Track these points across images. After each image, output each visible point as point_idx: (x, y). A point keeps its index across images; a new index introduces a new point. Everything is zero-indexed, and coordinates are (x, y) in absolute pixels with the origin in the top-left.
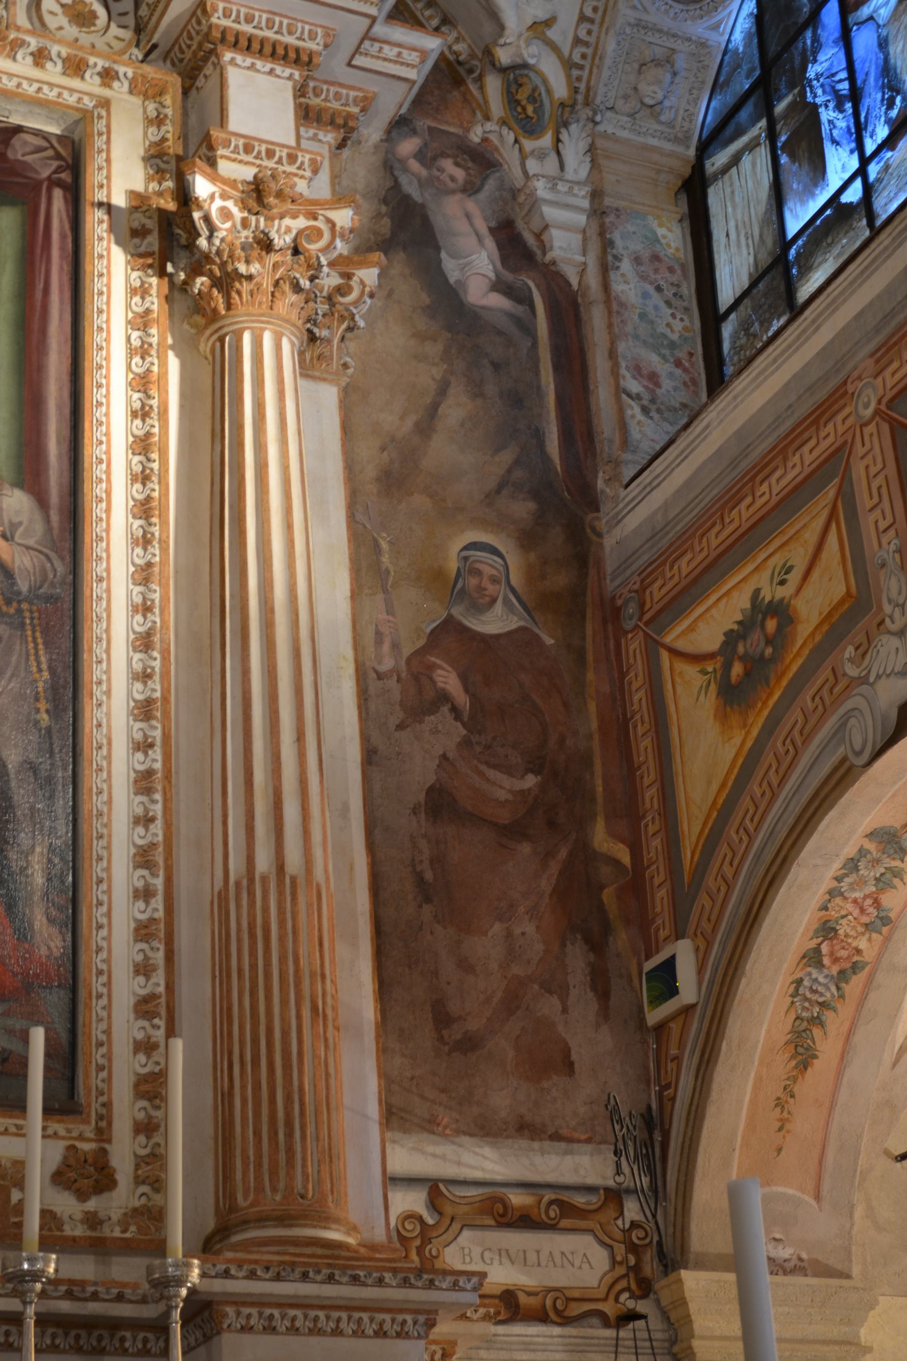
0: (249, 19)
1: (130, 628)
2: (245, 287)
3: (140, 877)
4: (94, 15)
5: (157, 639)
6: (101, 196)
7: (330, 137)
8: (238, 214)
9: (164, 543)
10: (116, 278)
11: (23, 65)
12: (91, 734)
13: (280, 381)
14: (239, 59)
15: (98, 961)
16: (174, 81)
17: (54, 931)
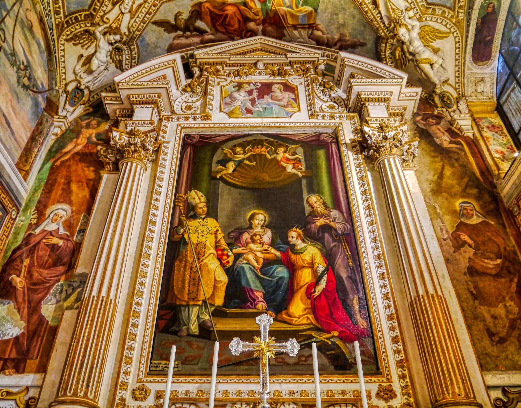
0: (370, 94)
1: (370, 237)
2: (383, 149)
3: (386, 303)
4: (335, 107)
5: (378, 238)
6: (344, 142)
7: (398, 118)
8: (377, 134)
9: (375, 215)
10: (351, 158)
11: (320, 120)
12: (364, 266)
13: (397, 168)
14: (370, 103)
15: (378, 328)
16: (356, 115)
17: (364, 321)
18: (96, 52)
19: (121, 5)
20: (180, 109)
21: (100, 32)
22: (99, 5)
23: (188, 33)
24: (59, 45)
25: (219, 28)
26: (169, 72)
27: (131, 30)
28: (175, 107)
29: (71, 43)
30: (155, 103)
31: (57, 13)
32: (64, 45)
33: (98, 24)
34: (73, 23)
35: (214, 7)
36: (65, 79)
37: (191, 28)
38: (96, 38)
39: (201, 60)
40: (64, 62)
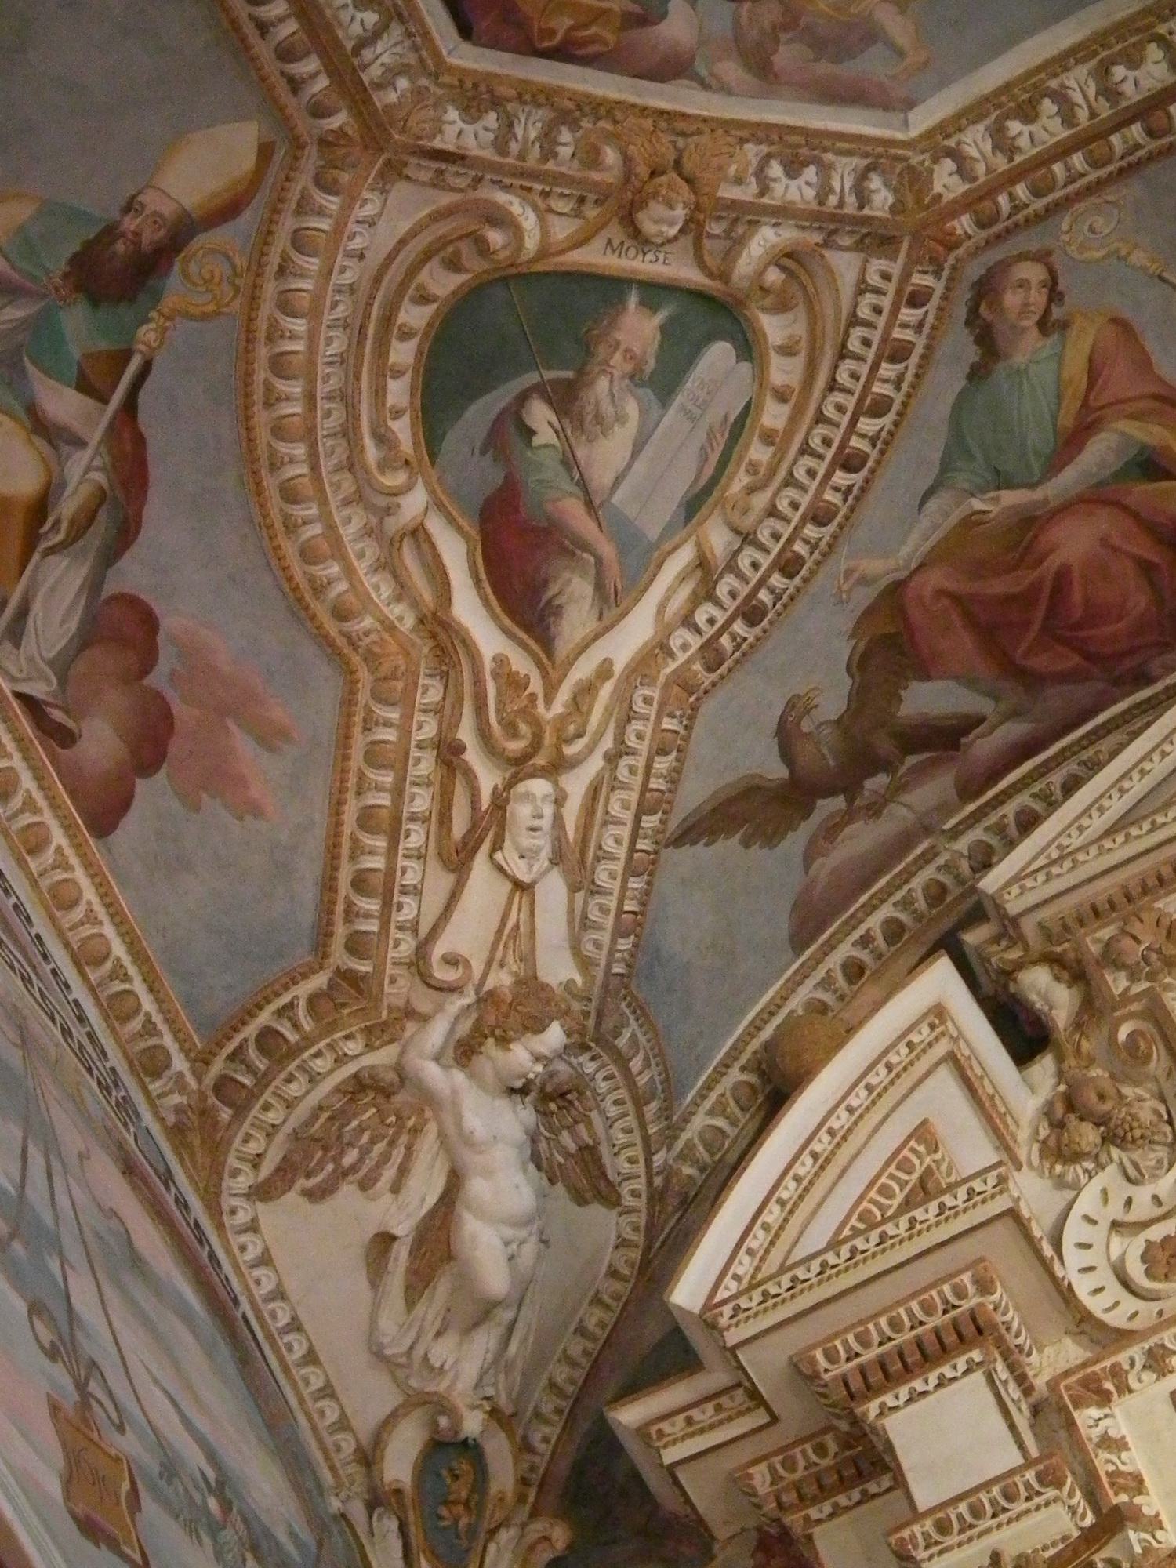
18: (455, 1181)
19: (497, 846)
20: (1115, 1290)
21: (437, 1059)
22: (372, 905)
23: (878, 782)
24: (236, 1240)
25: (1040, 662)
26: (942, 1100)
27: (588, 948)
28: (1082, 1287)
29: (292, 1197)
30: (975, 1330)
31: (152, 1064)
32: (253, 1227)
33: (410, 1013)
34: (263, 1080)
35: (979, 569)
36: (343, 1424)
37: (884, 745)
38: (428, 1099)
39: (1043, 914)
40: (295, 1325)
